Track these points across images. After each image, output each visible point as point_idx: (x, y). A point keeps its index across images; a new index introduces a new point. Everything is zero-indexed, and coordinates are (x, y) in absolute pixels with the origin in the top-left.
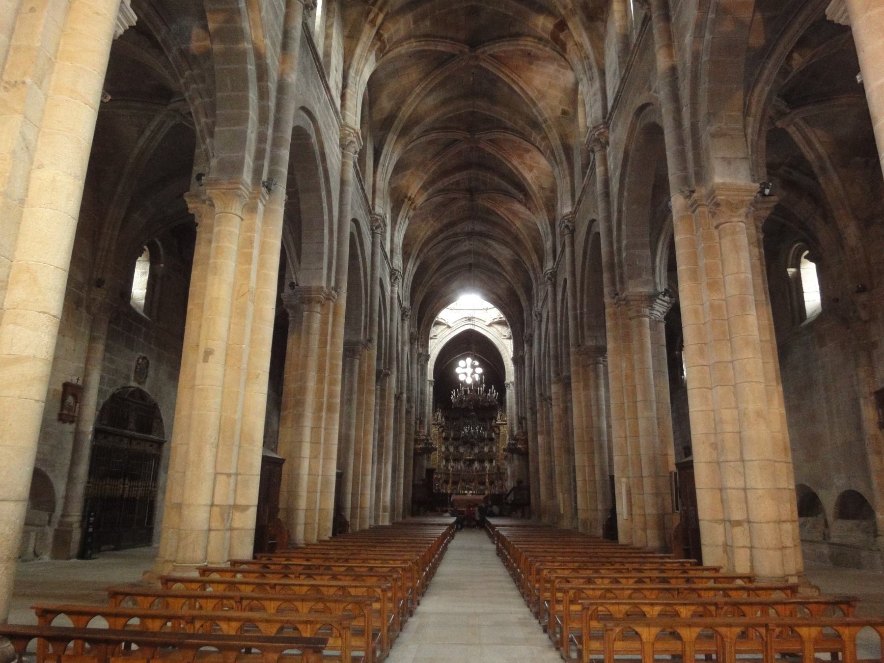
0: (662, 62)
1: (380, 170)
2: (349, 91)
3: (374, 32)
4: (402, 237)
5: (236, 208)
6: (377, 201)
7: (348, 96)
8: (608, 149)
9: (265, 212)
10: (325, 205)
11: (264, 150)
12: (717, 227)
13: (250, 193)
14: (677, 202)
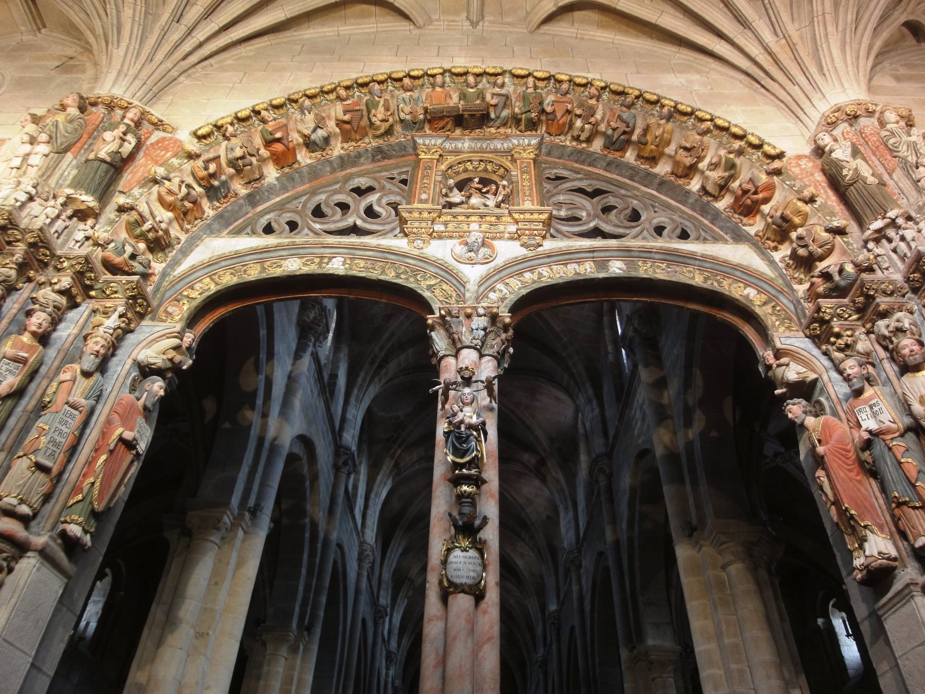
0: (609, 535)
1: (386, 562)
2: (369, 512)
3: (392, 463)
4: (400, 617)
5: (284, 651)
6: (382, 593)
7: (368, 516)
8: (582, 571)
9: (304, 650)
10: (341, 616)
11: (309, 597)
12: (653, 680)
13: (295, 636)
14: (624, 653)
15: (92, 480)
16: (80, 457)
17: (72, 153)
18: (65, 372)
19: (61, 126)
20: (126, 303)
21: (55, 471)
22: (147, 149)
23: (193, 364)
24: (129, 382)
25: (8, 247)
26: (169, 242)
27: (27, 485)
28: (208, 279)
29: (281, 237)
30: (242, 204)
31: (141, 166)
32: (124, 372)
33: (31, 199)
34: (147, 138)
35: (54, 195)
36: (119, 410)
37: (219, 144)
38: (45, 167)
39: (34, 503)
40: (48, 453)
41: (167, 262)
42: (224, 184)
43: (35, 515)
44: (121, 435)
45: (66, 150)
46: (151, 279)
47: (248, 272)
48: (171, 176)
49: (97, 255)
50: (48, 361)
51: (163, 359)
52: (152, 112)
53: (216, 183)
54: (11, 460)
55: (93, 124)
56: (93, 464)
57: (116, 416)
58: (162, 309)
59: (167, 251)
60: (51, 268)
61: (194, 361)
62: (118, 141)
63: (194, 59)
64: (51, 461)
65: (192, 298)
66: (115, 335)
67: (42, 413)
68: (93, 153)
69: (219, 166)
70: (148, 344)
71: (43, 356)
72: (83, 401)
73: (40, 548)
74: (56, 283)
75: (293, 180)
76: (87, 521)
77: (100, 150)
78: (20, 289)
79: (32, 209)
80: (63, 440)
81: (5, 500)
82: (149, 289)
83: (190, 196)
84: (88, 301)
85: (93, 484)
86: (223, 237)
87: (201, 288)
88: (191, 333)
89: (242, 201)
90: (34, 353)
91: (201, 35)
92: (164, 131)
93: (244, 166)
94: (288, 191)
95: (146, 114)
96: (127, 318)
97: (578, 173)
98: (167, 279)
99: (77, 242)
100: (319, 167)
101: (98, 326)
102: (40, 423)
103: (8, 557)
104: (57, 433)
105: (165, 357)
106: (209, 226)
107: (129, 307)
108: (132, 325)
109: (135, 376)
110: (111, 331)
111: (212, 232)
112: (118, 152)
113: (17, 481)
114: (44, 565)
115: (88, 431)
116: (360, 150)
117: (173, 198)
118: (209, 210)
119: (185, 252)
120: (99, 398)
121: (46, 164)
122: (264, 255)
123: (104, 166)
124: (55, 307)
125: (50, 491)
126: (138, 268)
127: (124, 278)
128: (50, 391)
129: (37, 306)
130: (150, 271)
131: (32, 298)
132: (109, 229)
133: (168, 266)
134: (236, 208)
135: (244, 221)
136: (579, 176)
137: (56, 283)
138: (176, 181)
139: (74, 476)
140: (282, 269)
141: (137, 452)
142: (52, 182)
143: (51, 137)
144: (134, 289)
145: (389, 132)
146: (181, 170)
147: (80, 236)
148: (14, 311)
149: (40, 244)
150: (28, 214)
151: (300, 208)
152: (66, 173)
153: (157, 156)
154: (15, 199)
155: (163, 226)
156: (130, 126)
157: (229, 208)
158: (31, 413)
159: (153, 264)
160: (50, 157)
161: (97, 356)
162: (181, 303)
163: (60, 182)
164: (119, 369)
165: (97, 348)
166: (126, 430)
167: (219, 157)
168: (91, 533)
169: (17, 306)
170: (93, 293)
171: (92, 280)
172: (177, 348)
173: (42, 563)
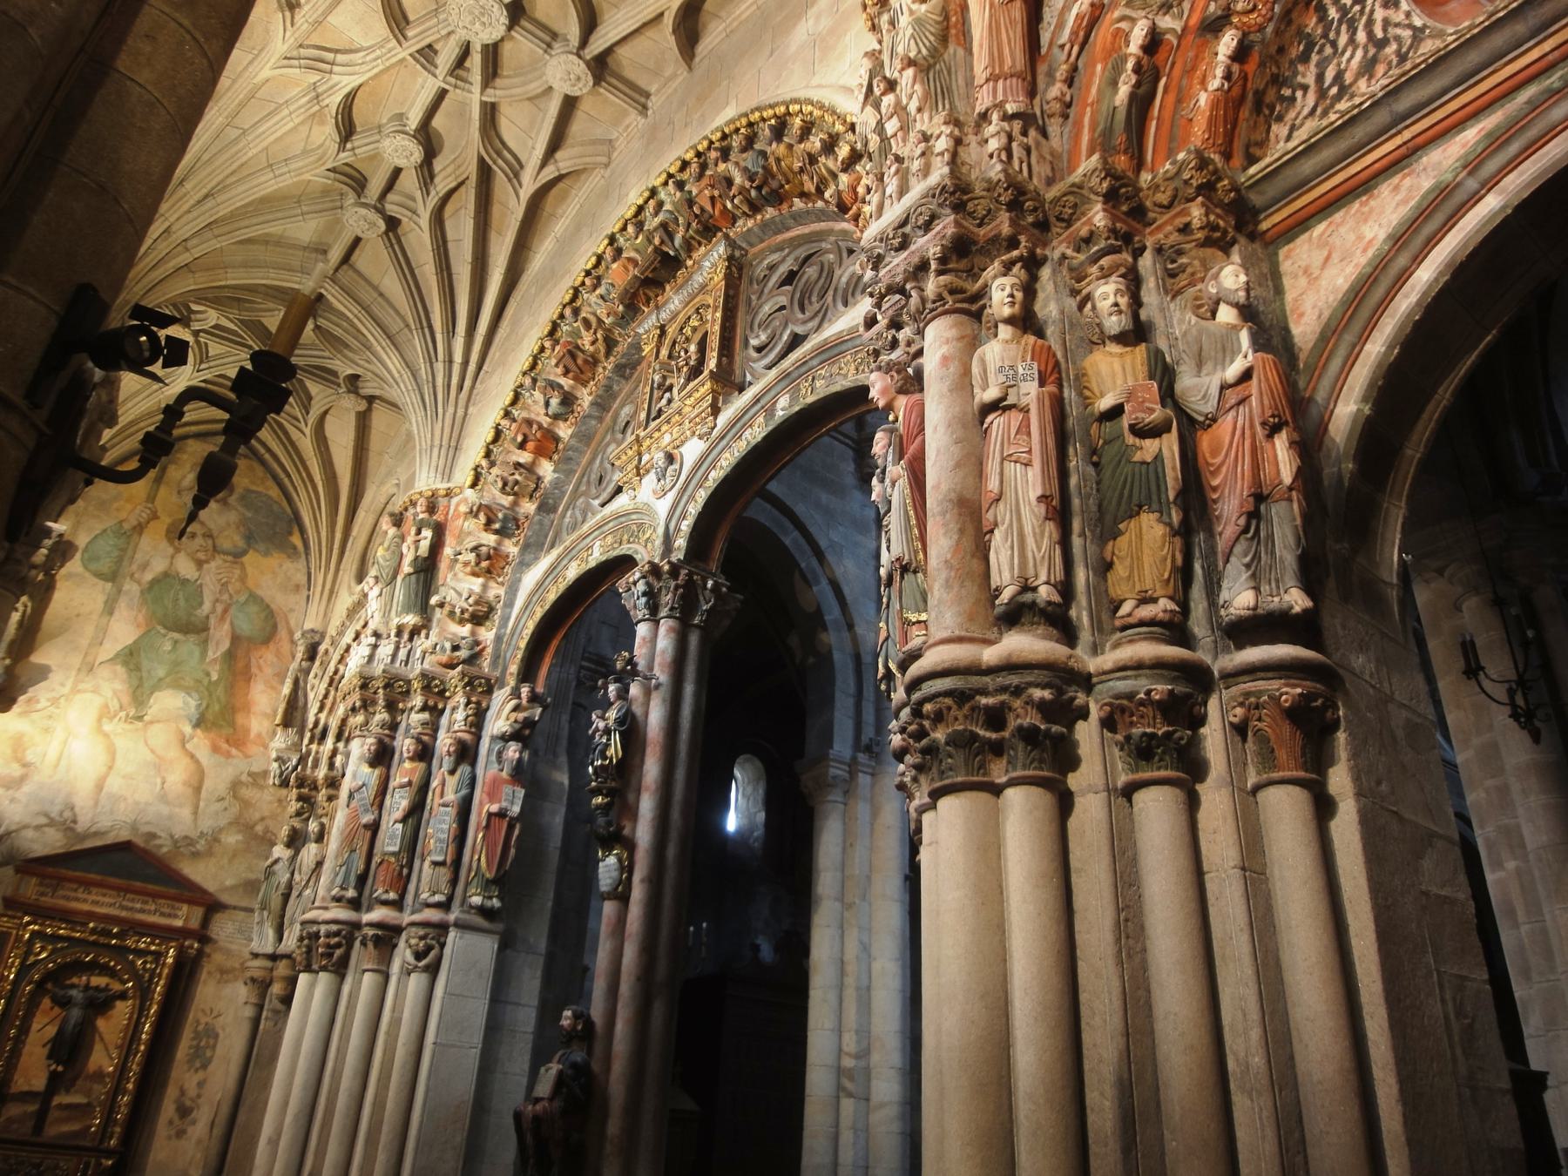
33: (375, 647)
53: (497, 526)
63: (468, 383)
75: (571, 459)
89: (537, 518)
91: (458, 358)
94: (576, 471)
97: (782, 249)
100: (583, 428)
108: (484, 705)
112: (416, 558)
116: (604, 382)
118: (511, 548)
119: (510, 604)
123: (413, 577)
133: (499, 629)
134: (537, 527)
136: (787, 251)
145: (610, 344)
157: (530, 533)
170: (447, 694)
172: (516, 709)
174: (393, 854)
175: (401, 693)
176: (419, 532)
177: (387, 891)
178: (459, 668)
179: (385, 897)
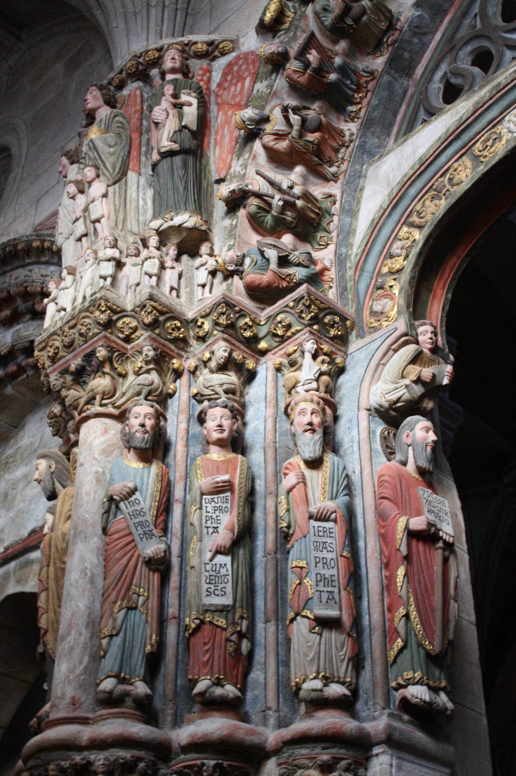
15: (402, 611)
16: (370, 585)
17: (133, 170)
18: (286, 474)
19: (99, 144)
20: (310, 332)
21: (347, 620)
22: (217, 96)
23: (454, 369)
24: (378, 445)
25: (129, 347)
26: (320, 209)
27: (322, 655)
28: (405, 229)
29: (475, 92)
30: (390, 83)
31: (223, 127)
32: (364, 435)
33: (119, 265)
34: (209, 81)
35: (142, 240)
36: (387, 492)
37: (304, 16)
38: (112, 212)
39: (345, 677)
40: (324, 600)
41: (334, 239)
42: (343, 70)
43: (355, 692)
44: (407, 527)
45: (123, 173)
46: (325, 278)
47: (455, 181)
48: (266, 112)
49: (237, 289)
50: (259, 470)
51: (407, 386)
52: (193, 38)
53: (333, 77)
54: (286, 628)
55: (135, 113)
56: (392, 588)
57: (386, 503)
58: (366, 313)
59: (324, 224)
60: (193, 342)
61: (454, 365)
62: (172, 112)
64: (333, 609)
65: (399, 271)
66: (322, 389)
67: (289, 546)
68: (155, 151)
69: (321, 49)
70: (373, 376)
71: (249, 468)
72: (330, 505)
73: (383, 737)
74: (210, 359)
76: (428, 673)
77: (159, 142)
78: (175, 392)
79: (128, 277)
80: (334, 572)
81: (305, 686)
82: (332, 295)
83: (307, 124)
84: (263, 360)
85: (407, 616)
86: (389, 152)
87: (402, 248)
88: (424, 324)
89: (386, 78)
90: (235, 469)
92: (223, 54)
93: (357, 20)
94: (445, 12)
95: (187, 48)
96: (325, 354)
98: (348, 265)
99: (203, 286)
101: (294, 387)
102: (293, 562)
103: (350, 764)
104: (320, 565)
105: (407, 381)
106: (362, 147)
107: (318, 337)
108: (339, 360)
109: (382, 433)
110: (314, 385)
111: (371, 155)
113: (307, 655)
114: (404, 760)
115: (361, 544)
117: (287, 141)
120: (349, 489)
121: (112, 207)
122: (465, 138)
123: (178, 160)
124: (226, 392)
125: (356, 650)
126: (299, 273)
127: (289, 299)
128: (282, 512)
129: (206, 403)
130: (318, 268)
131: (195, 396)
132: (232, 243)
135: (408, 106)
137: (210, 359)
138: (277, 114)
139: (376, 617)
140: (504, 141)
141: (445, 542)
142: (132, 225)
143: (97, 168)
144: (309, 307)
146: (275, 93)
147: (202, 276)
148: (183, 426)
149: (161, 318)
150: (128, 287)
151: (479, 25)
152: (141, 202)
153: (234, 97)
154: (101, 277)
155: (297, 190)
156: (176, 80)
157: (375, 102)
158: (276, 553)
159: (316, 255)
160: (110, 195)
161: (314, 431)
162: (386, 286)
163: (141, 218)
164: (355, 432)
165: (307, 419)
166: (411, 516)
167: (312, 35)
168: (444, 689)
169: (183, 418)
170: (263, 345)
171: (250, 327)
173: (399, 758)
174: (222, 610)
175: (175, 341)
176: (175, 96)
177: (218, 683)
178: (302, 289)
179: (218, 691)
